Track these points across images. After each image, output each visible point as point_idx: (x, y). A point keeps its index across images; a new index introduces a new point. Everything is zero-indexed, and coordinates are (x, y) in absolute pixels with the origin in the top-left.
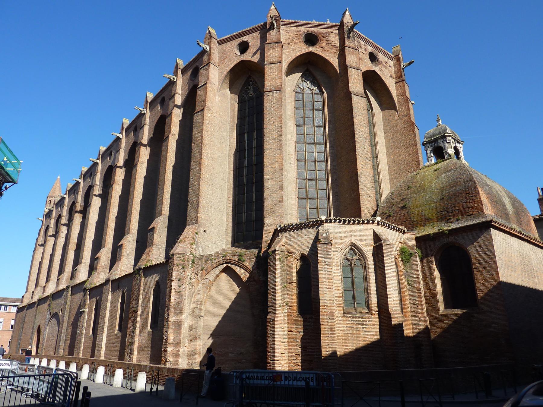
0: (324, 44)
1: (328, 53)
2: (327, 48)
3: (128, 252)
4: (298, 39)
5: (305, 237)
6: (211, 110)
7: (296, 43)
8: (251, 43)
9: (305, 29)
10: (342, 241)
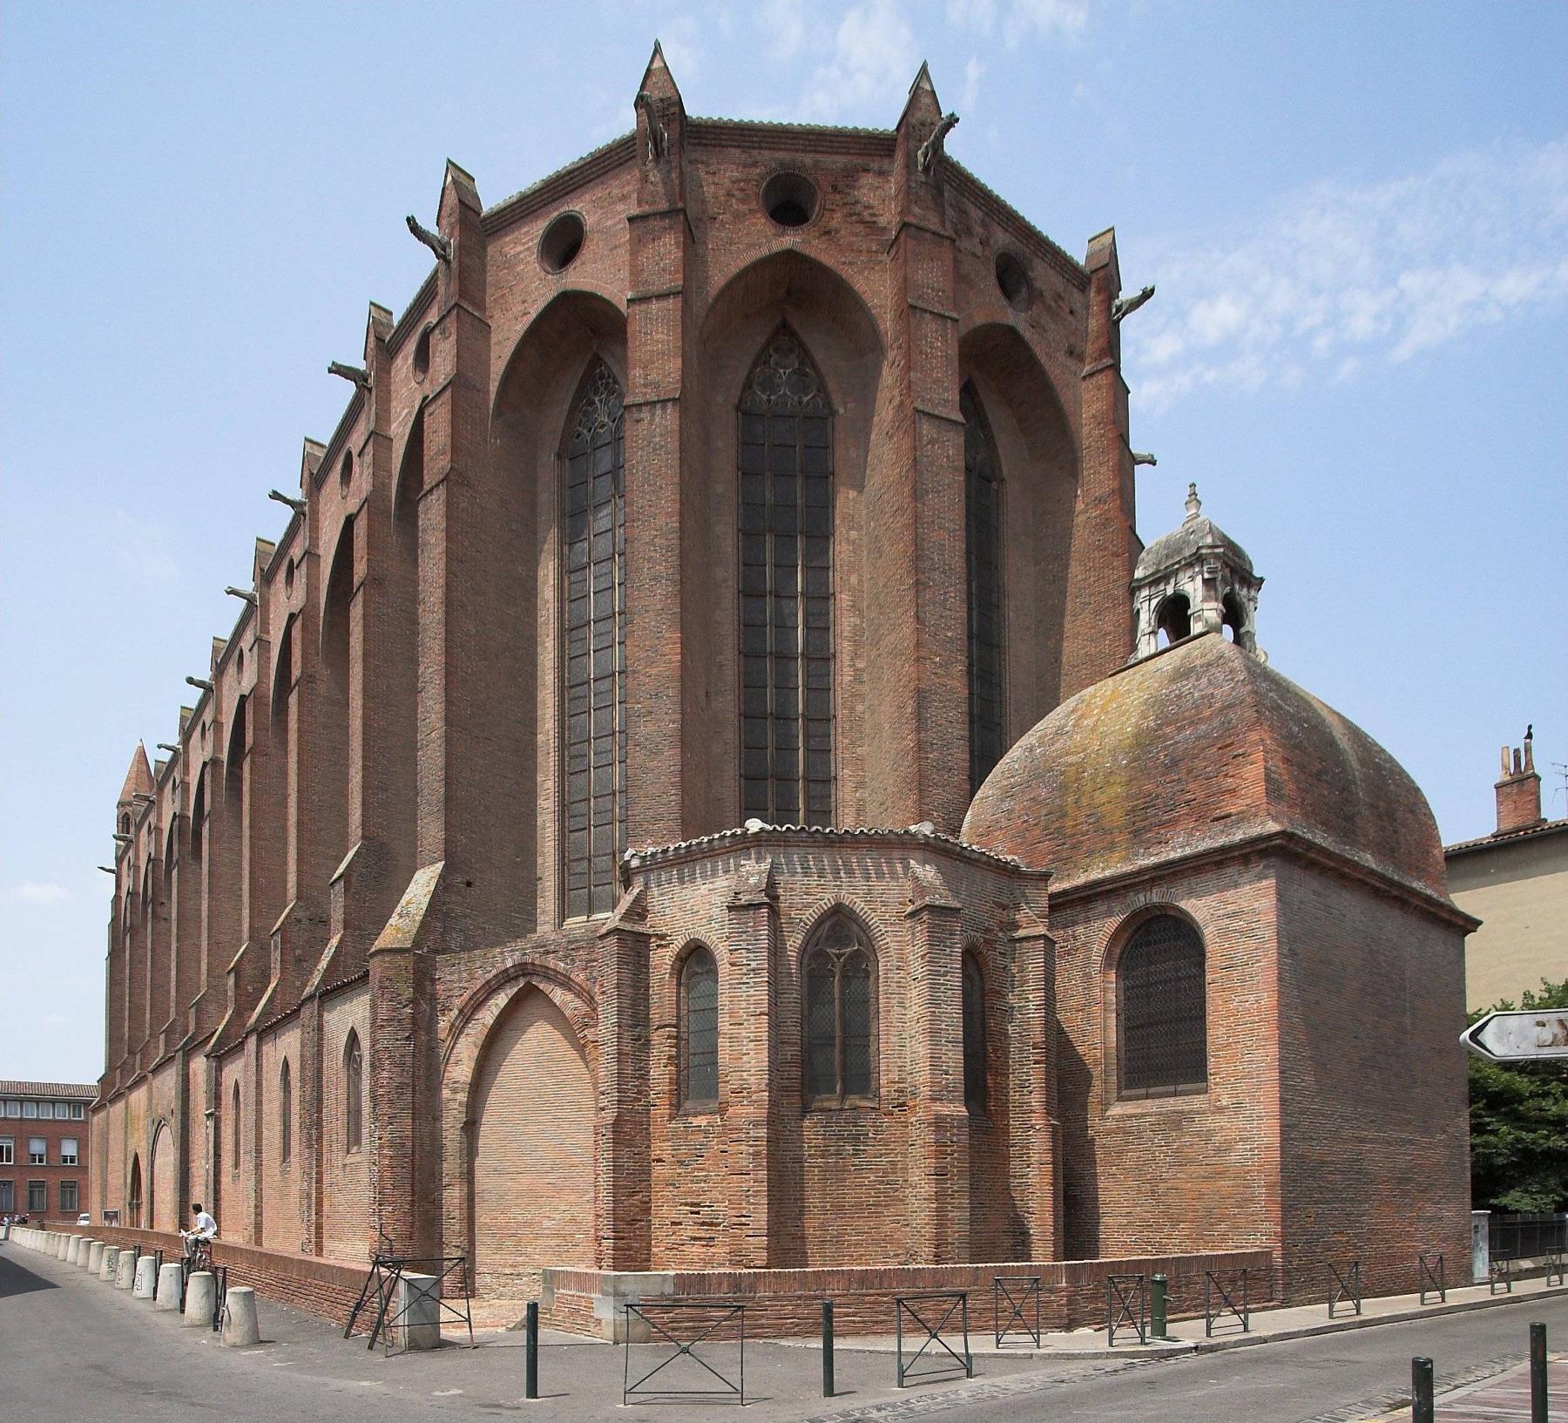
1: (850, 257)
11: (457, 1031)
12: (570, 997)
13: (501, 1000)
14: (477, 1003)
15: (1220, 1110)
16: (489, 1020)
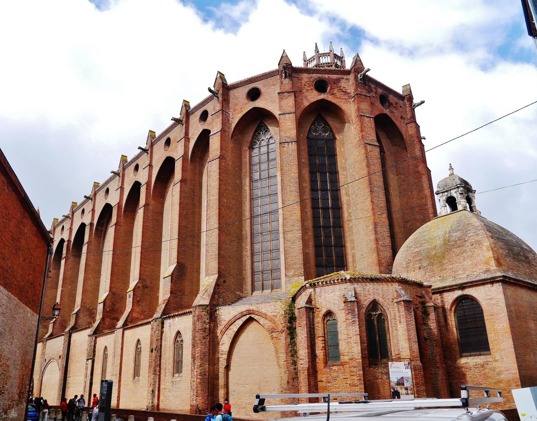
0: (336, 91)
1: (340, 100)
2: (338, 94)
3: (138, 298)
6: (225, 159)
7: (307, 90)
8: (263, 90)
9: (315, 76)
10: (366, 298)
11: (223, 333)
12: (266, 321)
13: (240, 323)
14: (231, 323)
15: (496, 361)
16: (236, 330)
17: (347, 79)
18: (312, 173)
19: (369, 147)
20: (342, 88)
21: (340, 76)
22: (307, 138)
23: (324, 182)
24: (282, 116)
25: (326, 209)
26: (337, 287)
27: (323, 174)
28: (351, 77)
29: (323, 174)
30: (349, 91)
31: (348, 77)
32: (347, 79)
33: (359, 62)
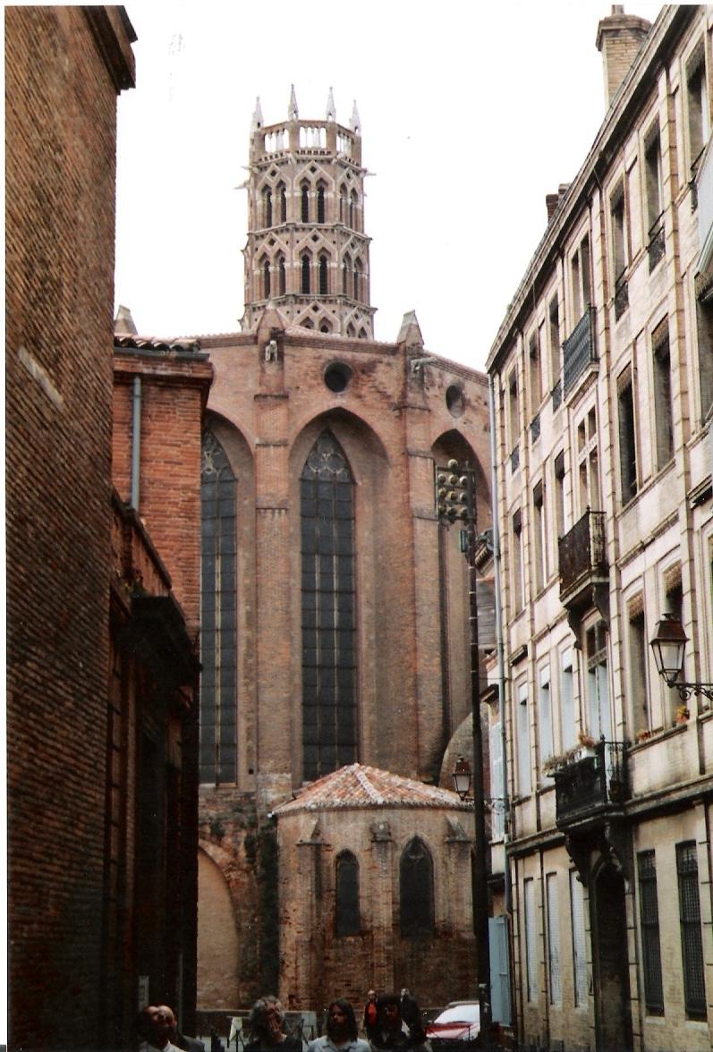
0: (364, 391)
2: (370, 398)
4: (315, 378)
5: (351, 825)
7: (311, 387)
9: (329, 354)
12: (220, 851)
17: (389, 364)
18: (306, 554)
19: (419, 525)
20: (377, 383)
21: (375, 356)
22: (303, 480)
23: (327, 575)
24: (262, 451)
25: (326, 630)
26: (361, 814)
27: (327, 556)
28: (398, 362)
29: (327, 556)
30: (390, 391)
31: (391, 359)
32: (389, 364)
33: (416, 331)
